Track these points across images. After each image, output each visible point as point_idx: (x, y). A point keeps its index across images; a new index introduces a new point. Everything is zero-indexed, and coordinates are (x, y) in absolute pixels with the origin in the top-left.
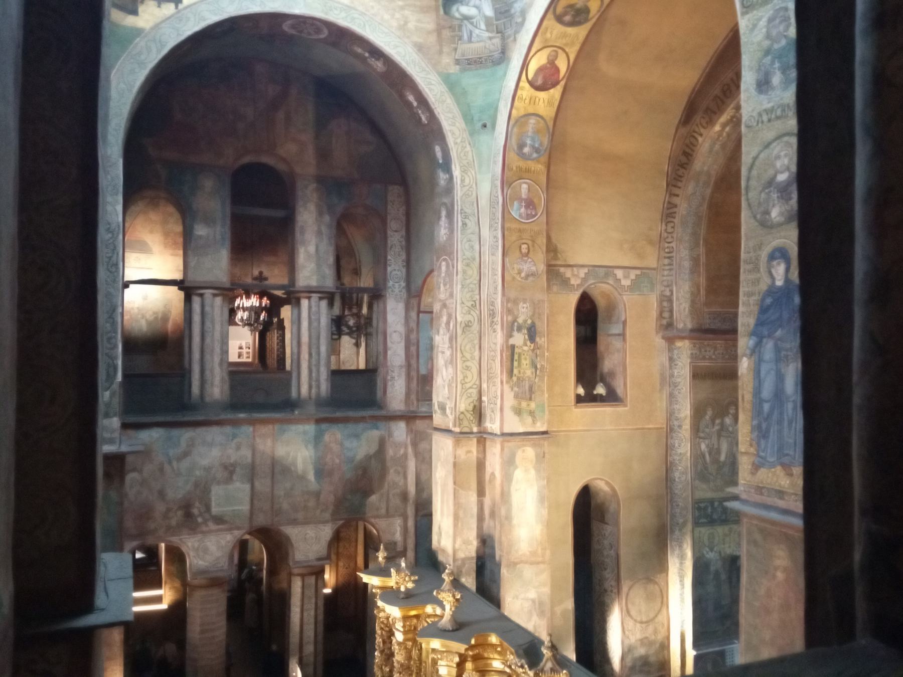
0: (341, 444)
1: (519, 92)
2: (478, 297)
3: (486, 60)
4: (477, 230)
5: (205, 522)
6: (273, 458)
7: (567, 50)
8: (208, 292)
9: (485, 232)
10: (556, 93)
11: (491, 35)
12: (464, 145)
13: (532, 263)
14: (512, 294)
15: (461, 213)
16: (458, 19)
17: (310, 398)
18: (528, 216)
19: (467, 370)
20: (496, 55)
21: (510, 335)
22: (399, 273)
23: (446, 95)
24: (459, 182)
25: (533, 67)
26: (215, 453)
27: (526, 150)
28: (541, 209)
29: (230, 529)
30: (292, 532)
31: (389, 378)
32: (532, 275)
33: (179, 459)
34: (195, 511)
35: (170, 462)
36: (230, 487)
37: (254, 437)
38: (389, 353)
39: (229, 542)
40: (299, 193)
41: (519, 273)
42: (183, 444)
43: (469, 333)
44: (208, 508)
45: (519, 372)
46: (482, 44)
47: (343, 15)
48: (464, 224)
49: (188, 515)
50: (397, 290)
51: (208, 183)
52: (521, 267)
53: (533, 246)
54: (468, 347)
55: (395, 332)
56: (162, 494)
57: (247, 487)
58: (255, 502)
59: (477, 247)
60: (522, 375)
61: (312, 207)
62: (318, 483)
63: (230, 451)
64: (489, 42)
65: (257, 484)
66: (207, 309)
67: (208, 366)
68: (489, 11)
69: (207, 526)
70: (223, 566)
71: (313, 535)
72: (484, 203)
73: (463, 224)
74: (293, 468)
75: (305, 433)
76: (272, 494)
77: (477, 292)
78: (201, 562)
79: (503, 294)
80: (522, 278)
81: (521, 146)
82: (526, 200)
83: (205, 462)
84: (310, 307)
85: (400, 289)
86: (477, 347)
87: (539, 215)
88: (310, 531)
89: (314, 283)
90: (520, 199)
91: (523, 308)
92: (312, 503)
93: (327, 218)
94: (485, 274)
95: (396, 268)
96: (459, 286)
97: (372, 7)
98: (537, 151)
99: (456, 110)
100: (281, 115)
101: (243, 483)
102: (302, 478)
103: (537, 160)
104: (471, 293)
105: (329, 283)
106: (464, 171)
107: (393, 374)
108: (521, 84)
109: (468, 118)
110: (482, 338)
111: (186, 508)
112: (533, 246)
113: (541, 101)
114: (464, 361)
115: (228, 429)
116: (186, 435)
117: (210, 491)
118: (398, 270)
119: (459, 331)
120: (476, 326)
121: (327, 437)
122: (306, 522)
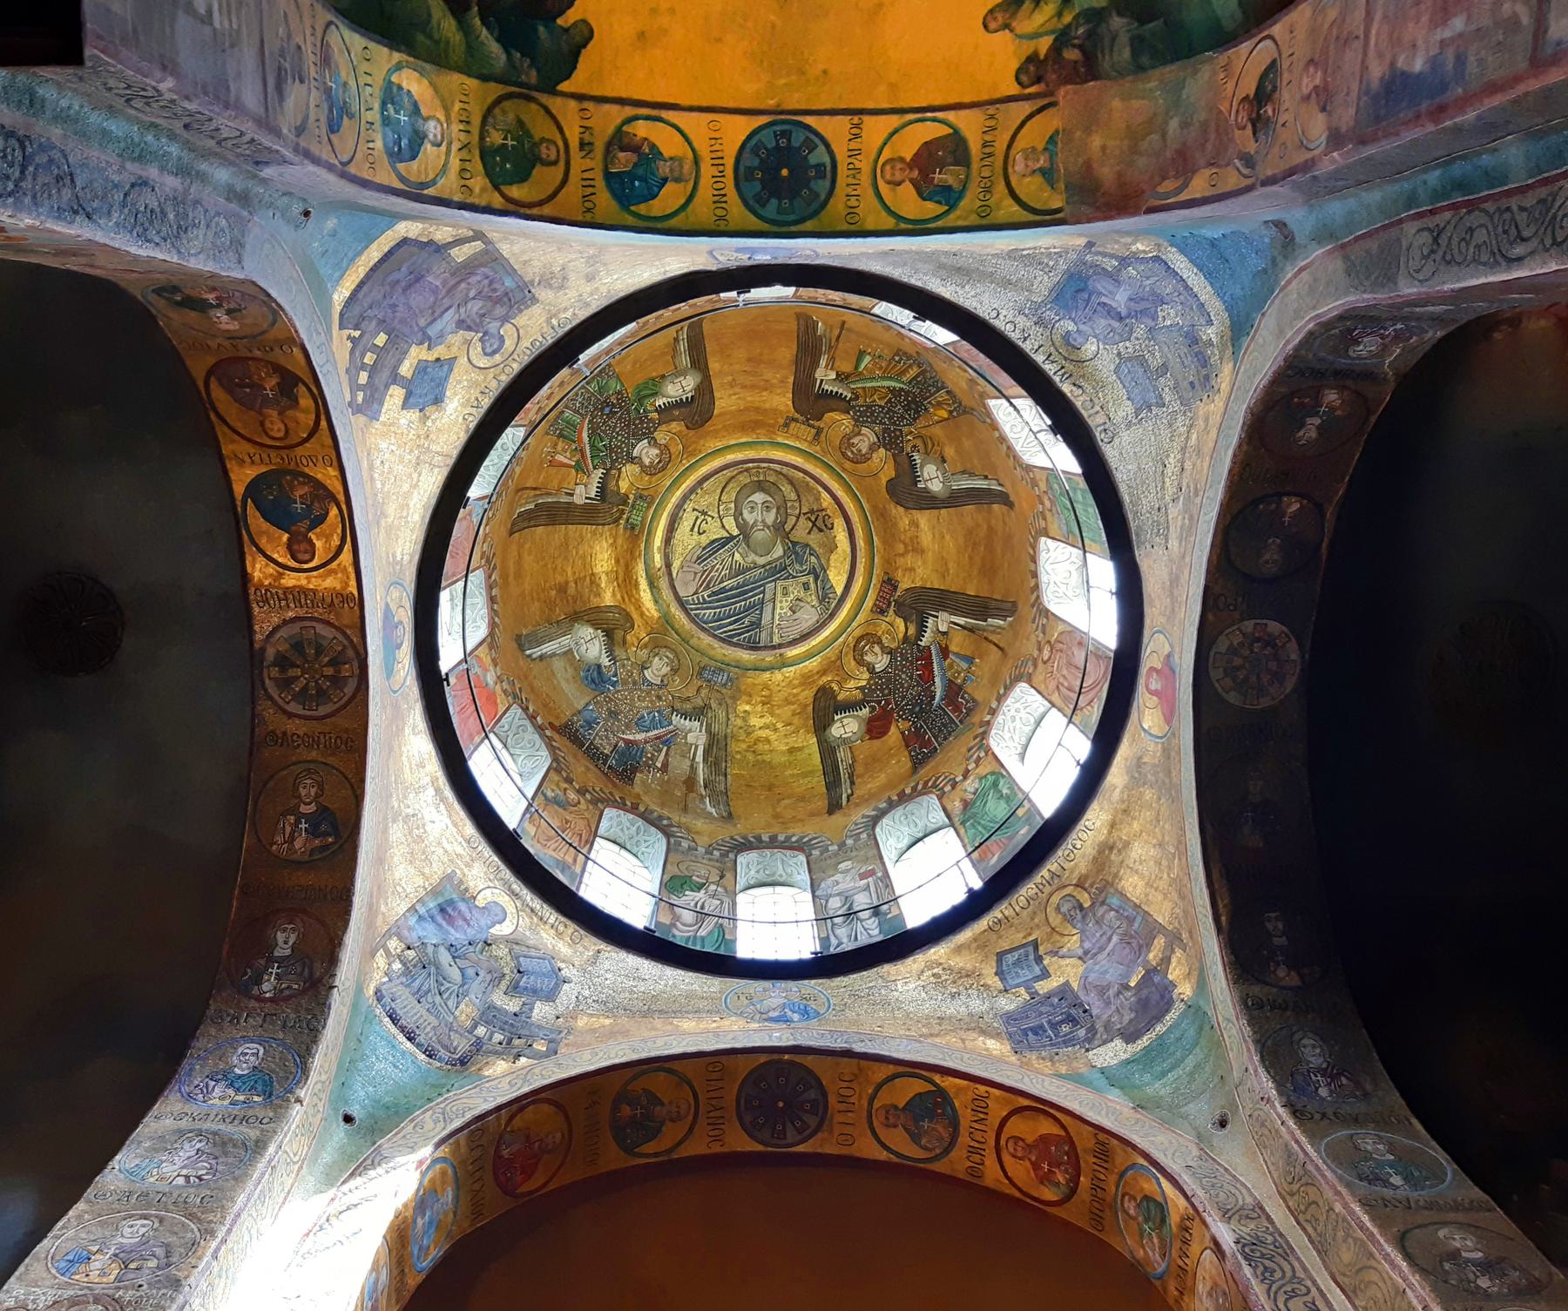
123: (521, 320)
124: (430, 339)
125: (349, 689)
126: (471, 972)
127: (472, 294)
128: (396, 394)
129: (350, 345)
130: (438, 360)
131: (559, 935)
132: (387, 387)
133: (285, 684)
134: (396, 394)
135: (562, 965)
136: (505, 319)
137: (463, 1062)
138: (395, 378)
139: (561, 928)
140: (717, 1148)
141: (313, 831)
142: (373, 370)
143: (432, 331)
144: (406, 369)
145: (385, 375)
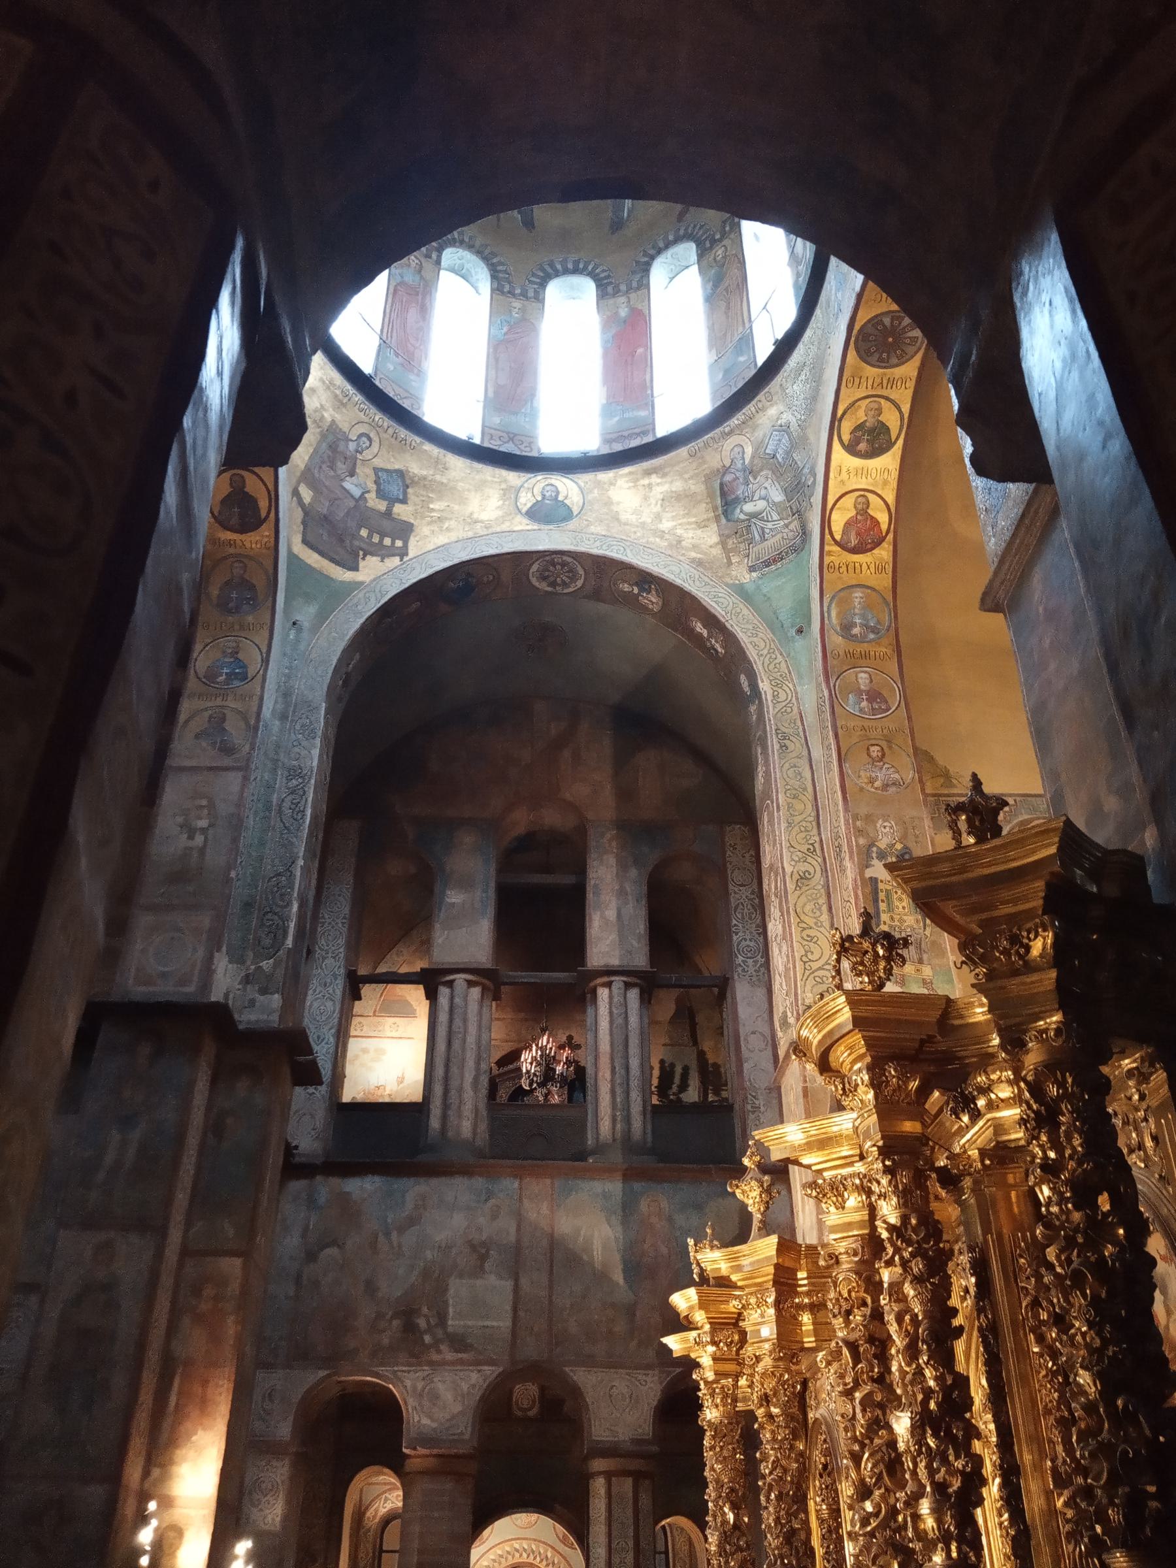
0: (670, 1220)
1: (827, 560)
2: (817, 839)
3: (787, 553)
4: (805, 753)
5: (437, 1343)
6: (552, 1236)
7: (880, 492)
8: (460, 978)
9: (817, 753)
10: (884, 553)
11: (786, 521)
12: (774, 656)
13: (893, 770)
14: (863, 810)
15: (777, 734)
16: (744, 521)
17: (614, 1140)
18: (874, 711)
19: (811, 941)
20: (798, 541)
21: (865, 864)
22: (752, 944)
23: (741, 606)
24: (770, 698)
25: (838, 521)
26: (458, 1221)
27: (856, 631)
28: (895, 700)
29: (477, 1363)
30: (585, 1378)
31: (749, 1107)
32: (894, 784)
33: (401, 1230)
34: (422, 1323)
35: (387, 1234)
36: (479, 1282)
37: (520, 1200)
38: (746, 1066)
39: (474, 1386)
40: (592, 844)
41: (872, 781)
42: (410, 1205)
43: (807, 888)
44: (442, 1318)
45: (892, 919)
46: (779, 536)
47: (598, 543)
48: (783, 747)
49: (410, 1328)
50: (751, 970)
51: (468, 839)
52: (873, 775)
53: (890, 748)
54: (808, 908)
55: (754, 1033)
56: (371, 1288)
57: (508, 1285)
58: (521, 1314)
59: (808, 774)
60: (897, 923)
61: (612, 860)
62: (630, 1287)
63: (482, 1220)
64: (786, 530)
65: (524, 1282)
66: (457, 1000)
67: (454, 1083)
68: (778, 496)
69: (439, 1352)
70: (462, 1433)
71: (625, 1391)
72: (811, 718)
73: (781, 747)
74: (585, 1257)
75: (606, 1196)
76: (551, 1301)
77: (815, 831)
78: (425, 1421)
79: (846, 810)
80: (876, 788)
81: (846, 628)
82: (868, 693)
83: (441, 1237)
84: (611, 997)
85: (757, 968)
86: (825, 908)
87: (894, 709)
88: (620, 1383)
89: (615, 961)
90: (859, 692)
91: (885, 827)
92: (620, 1327)
93: (633, 873)
94: (824, 808)
95: (746, 937)
96: (783, 825)
97: (635, 533)
98: (874, 630)
99: (756, 620)
100: (566, 753)
101: (501, 1278)
102: (601, 1277)
103: (877, 641)
104: (803, 835)
105: (640, 960)
106: (777, 685)
107: (757, 1102)
108: (827, 548)
109: (774, 625)
110: (832, 896)
111: (407, 1315)
112: (890, 748)
113: (864, 567)
114: (804, 929)
115: (479, 1182)
116: (414, 1189)
117: (446, 1290)
118: (750, 940)
119: (791, 886)
120: (818, 878)
121: (644, 1206)
122: (613, 1364)
123: (345, 427)
124: (363, 494)
125: (569, 560)
126: (763, 492)
127: (332, 473)
128: (398, 509)
129: (368, 557)
130: (375, 482)
131: (763, 409)
132: (394, 519)
133: (565, 584)
134: (398, 509)
135: (779, 422)
136: (348, 440)
137: (804, 533)
138: (388, 514)
139: (760, 405)
140: (911, 385)
141: (649, 592)
142: (383, 535)
143: (357, 492)
144: (382, 506)
145: (386, 524)
